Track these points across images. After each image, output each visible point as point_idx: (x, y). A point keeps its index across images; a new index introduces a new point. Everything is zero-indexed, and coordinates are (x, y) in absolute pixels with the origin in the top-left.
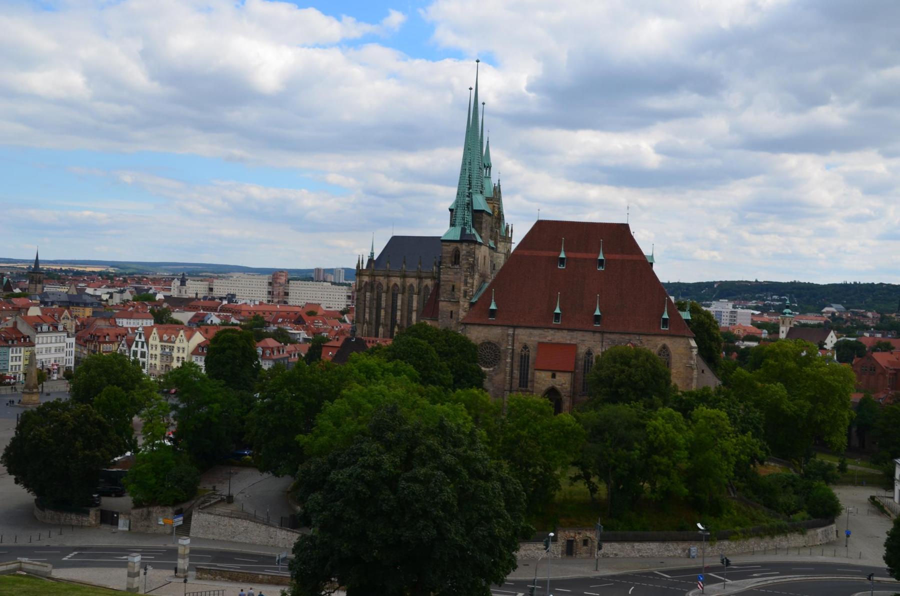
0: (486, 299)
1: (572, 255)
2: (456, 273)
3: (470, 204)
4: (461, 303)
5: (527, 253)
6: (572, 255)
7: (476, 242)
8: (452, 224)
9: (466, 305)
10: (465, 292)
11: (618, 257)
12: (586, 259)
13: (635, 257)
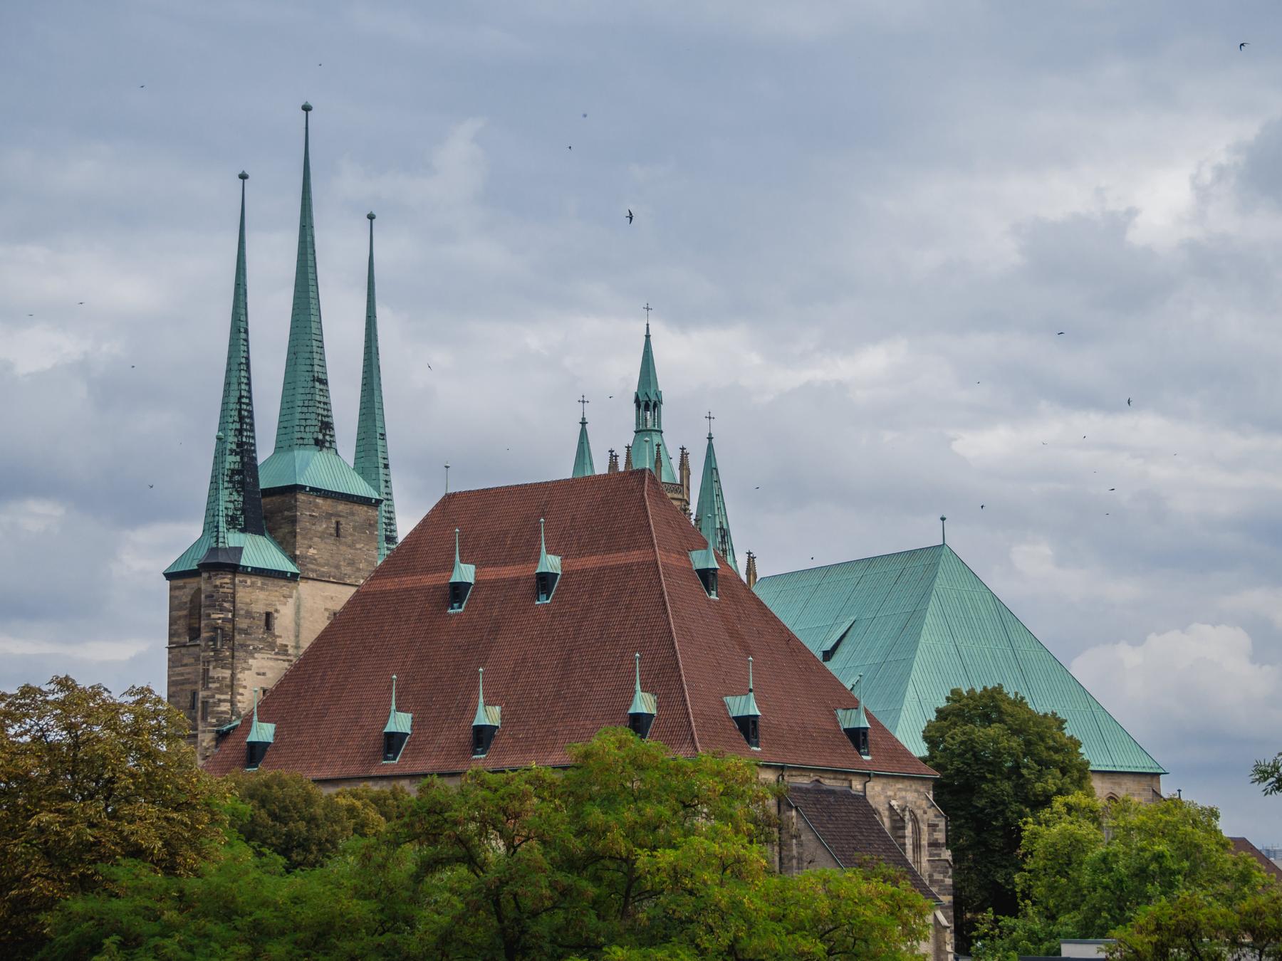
1: (491, 573)
5: (390, 584)
6: (491, 573)
7: (235, 569)
11: (591, 562)
12: (517, 580)
13: (635, 556)
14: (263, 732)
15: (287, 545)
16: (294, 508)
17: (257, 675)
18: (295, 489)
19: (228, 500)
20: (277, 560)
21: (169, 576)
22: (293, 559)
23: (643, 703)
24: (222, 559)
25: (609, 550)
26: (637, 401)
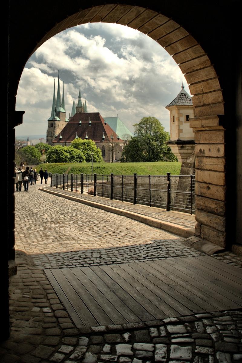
0: (59, 136)
2: (52, 129)
3: (56, 110)
4: (53, 137)
6: (83, 122)
7: (56, 120)
8: (51, 116)
9: (54, 137)
10: (54, 134)
11: (95, 122)
13: (99, 122)
14: (61, 137)
15: (59, 117)
16: (60, 114)
17: (58, 132)
18: (60, 112)
19: (55, 113)
20: (59, 120)
21: (48, 121)
22: (60, 119)
23: (104, 137)
24: (55, 119)
25: (97, 121)
26: (79, 97)
